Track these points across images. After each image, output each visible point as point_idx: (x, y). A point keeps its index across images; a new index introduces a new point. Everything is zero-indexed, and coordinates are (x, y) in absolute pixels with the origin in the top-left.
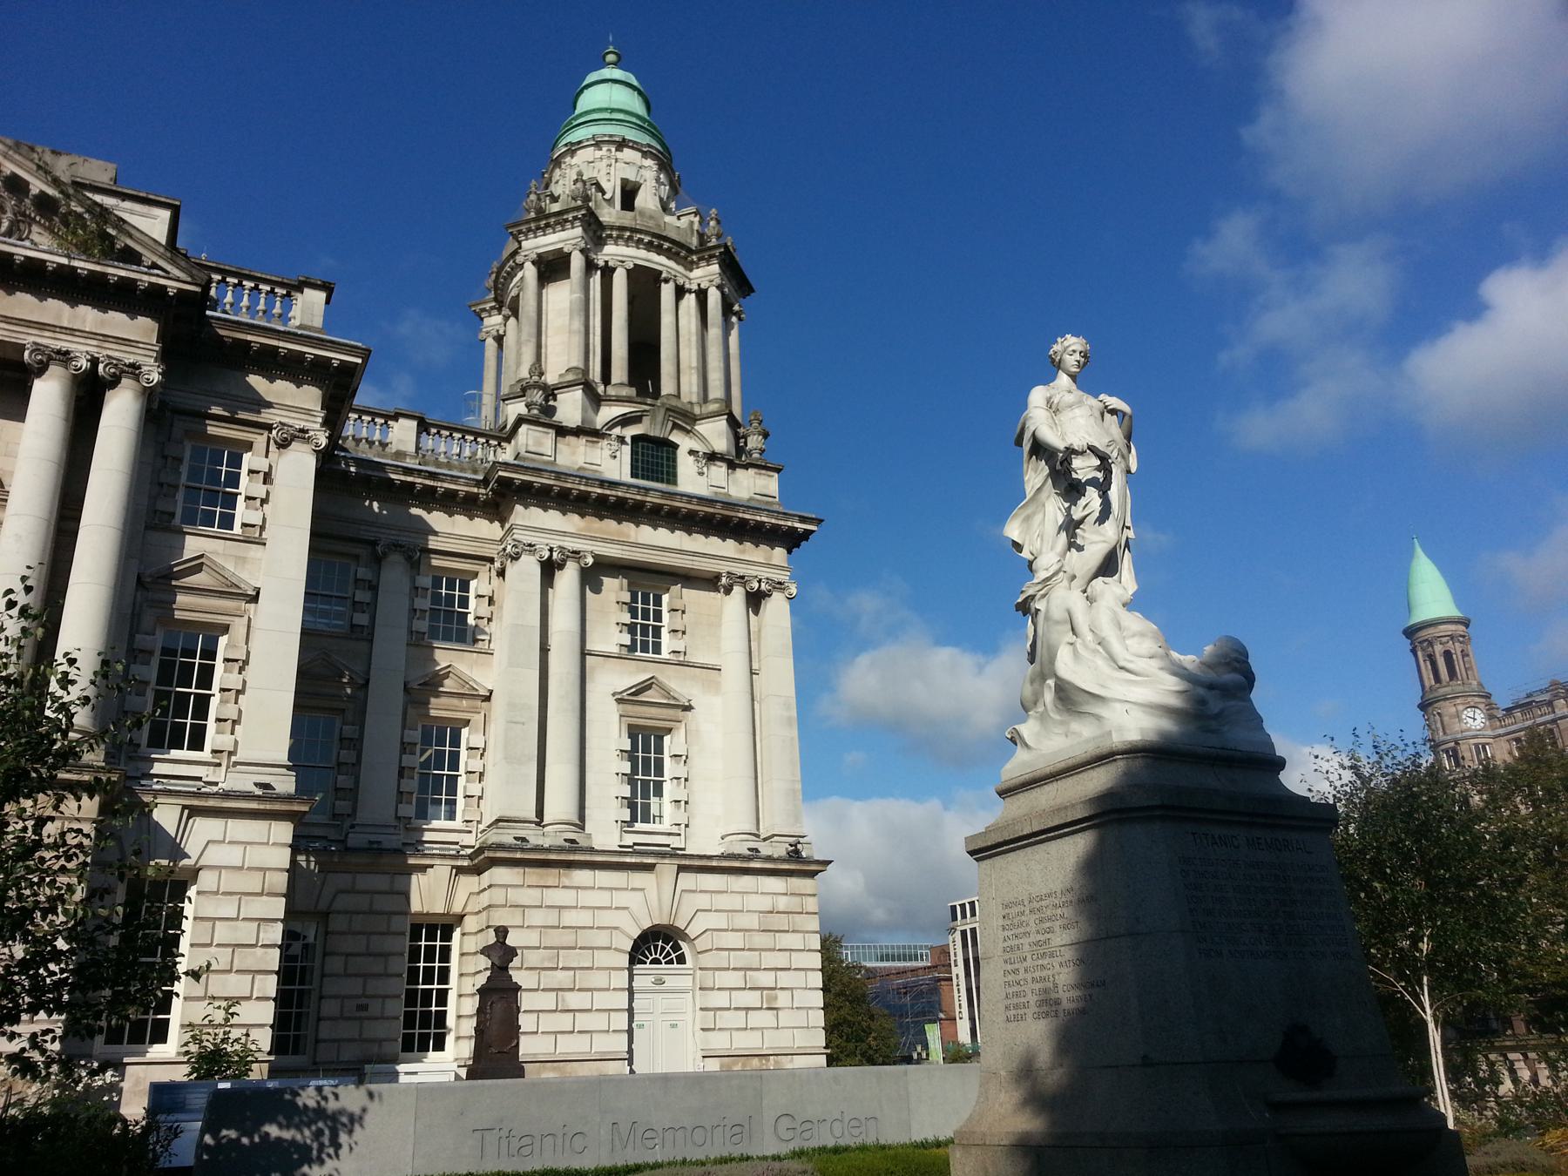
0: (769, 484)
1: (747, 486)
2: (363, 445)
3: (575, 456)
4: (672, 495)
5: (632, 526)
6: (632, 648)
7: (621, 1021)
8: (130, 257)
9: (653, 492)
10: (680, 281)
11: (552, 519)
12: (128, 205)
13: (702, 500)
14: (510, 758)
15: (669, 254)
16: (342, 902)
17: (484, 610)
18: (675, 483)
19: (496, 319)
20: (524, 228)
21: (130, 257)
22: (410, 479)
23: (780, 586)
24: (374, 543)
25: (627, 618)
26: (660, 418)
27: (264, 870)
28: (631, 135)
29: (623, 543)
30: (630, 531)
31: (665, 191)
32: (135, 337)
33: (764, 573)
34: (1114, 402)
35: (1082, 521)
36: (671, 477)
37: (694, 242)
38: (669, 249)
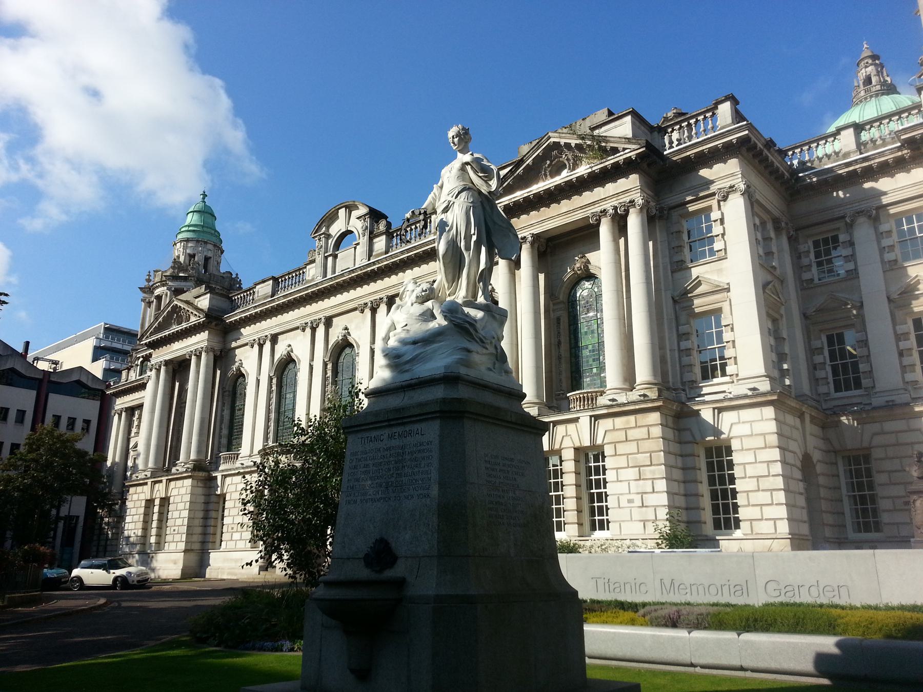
8: (615, 151)
12: (604, 129)
16: (877, 440)
21: (615, 151)
22: (851, 168)
24: (843, 217)
27: (764, 435)
32: (630, 186)
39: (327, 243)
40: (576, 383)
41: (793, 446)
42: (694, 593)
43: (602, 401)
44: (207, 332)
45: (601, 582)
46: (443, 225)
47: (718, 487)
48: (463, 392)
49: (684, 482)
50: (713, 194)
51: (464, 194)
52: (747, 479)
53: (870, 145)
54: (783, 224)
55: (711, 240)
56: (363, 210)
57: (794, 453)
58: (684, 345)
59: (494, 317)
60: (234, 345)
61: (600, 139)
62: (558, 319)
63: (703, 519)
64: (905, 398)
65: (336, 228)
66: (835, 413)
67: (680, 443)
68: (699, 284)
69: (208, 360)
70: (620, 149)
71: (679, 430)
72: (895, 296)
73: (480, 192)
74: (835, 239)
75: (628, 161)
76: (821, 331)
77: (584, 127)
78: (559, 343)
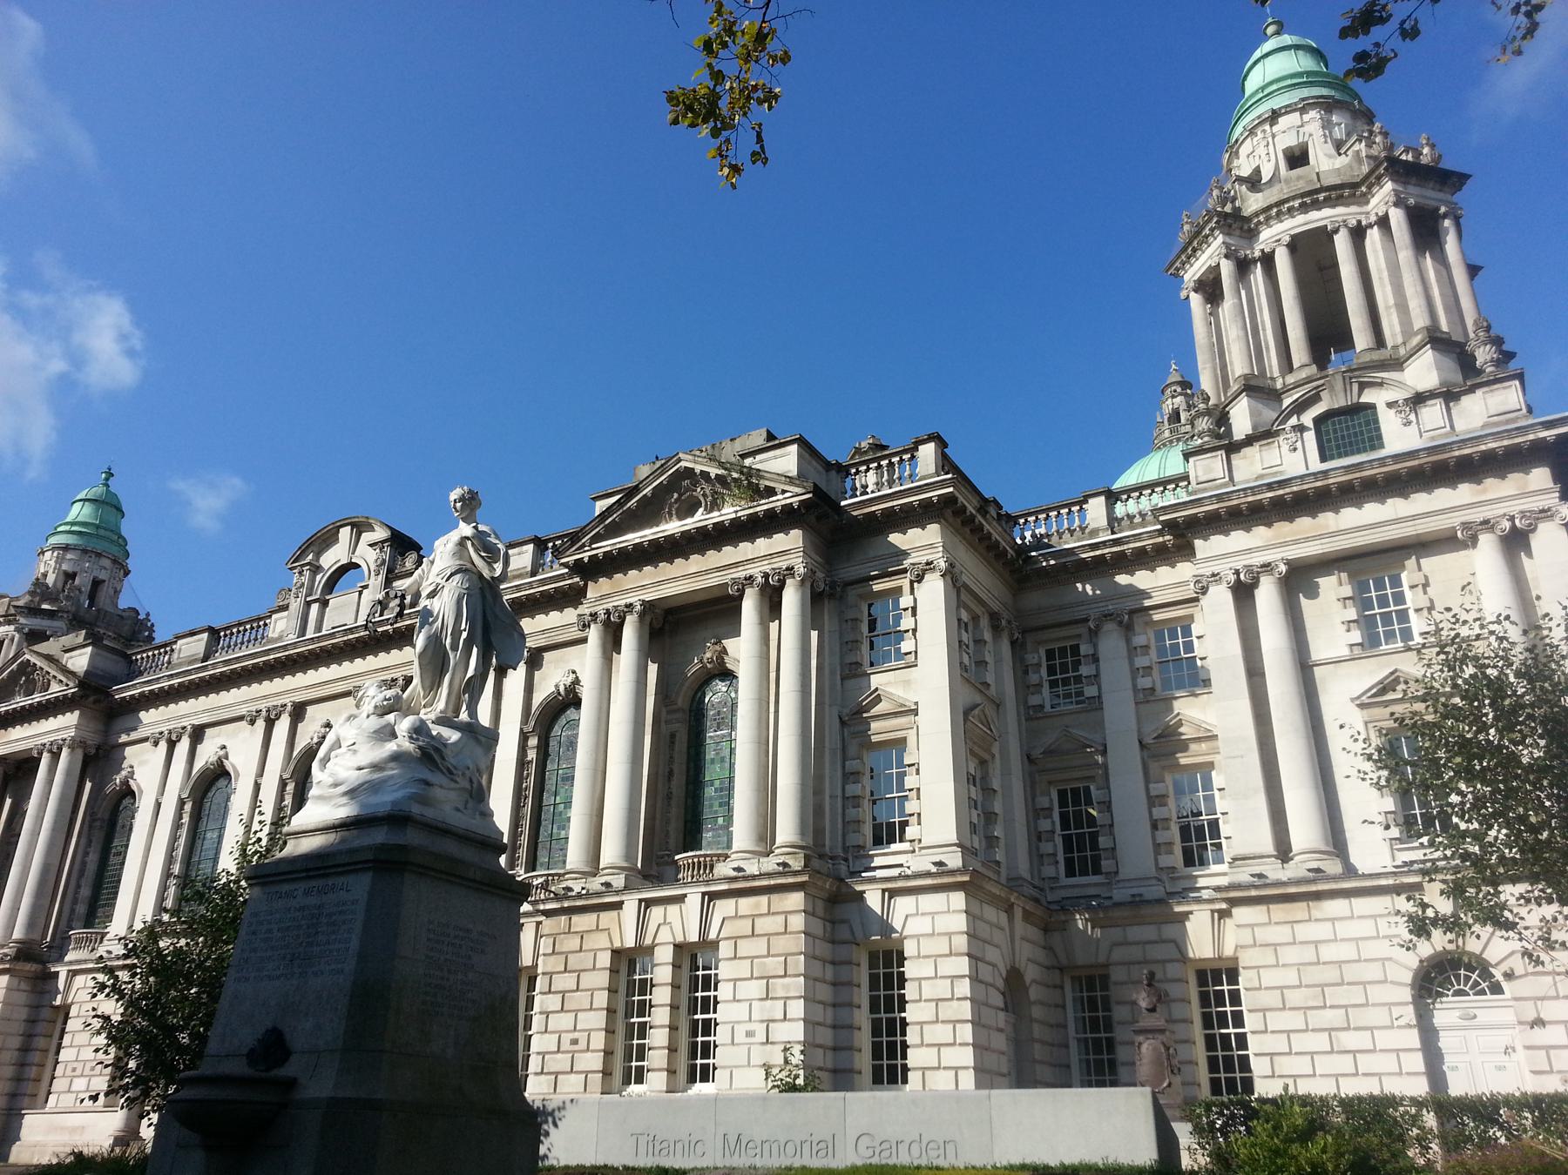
0: (1509, 397)
1: (1484, 412)
2: (1067, 536)
3: (1253, 466)
4: (1382, 461)
5: (1330, 515)
11: (1237, 540)
12: (759, 457)
15: (1330, 202)
16: (1118, 954)
18: (1382, 446)
21: (771, 492)
22: (1098, 553)
23: (1545, 514)
24: (1086, 620)
26: (1339, 385)
27: (950, 935)
29: (1321, 537)
32: (788, 546)
33: (1515, 507)
36: (1376, 441)
38: (1326, 199)
39: (312, 580)
40: (692, 838)
41: (992, 954)
42: (766, 1153)
43: (723, 869)
44: (77, 713)
45: (643, 1140)
46: (426, 615)
47: (883, 1015)
48: (412, 837)
49: (834, 1005)
50: (905, 571)
51: (457, 577)
52: (923, 1004)
53: (1126, 523)
54: (1004, 622)
55: (900, 635)
56: (380, 534)
57: (994, 966)
58: (852, 789)
59: (478, 741)
60: (124, 738)
61: (750, 473)
62: (673, 736)
63: (857, 1066)
64: (1155, 892)
65: (332, 558)
66: (1063, 909)
67: (833, 942)
68: (878, 700)
69: (71, 763)
70: (778, 490)
71: (833, 922)
72: (1148, 740)
73: (481, 576)
74: (1075, 650)
75: (788, 509)
76: (1050, 783)
77: (730, 452)
78: (671, 773)
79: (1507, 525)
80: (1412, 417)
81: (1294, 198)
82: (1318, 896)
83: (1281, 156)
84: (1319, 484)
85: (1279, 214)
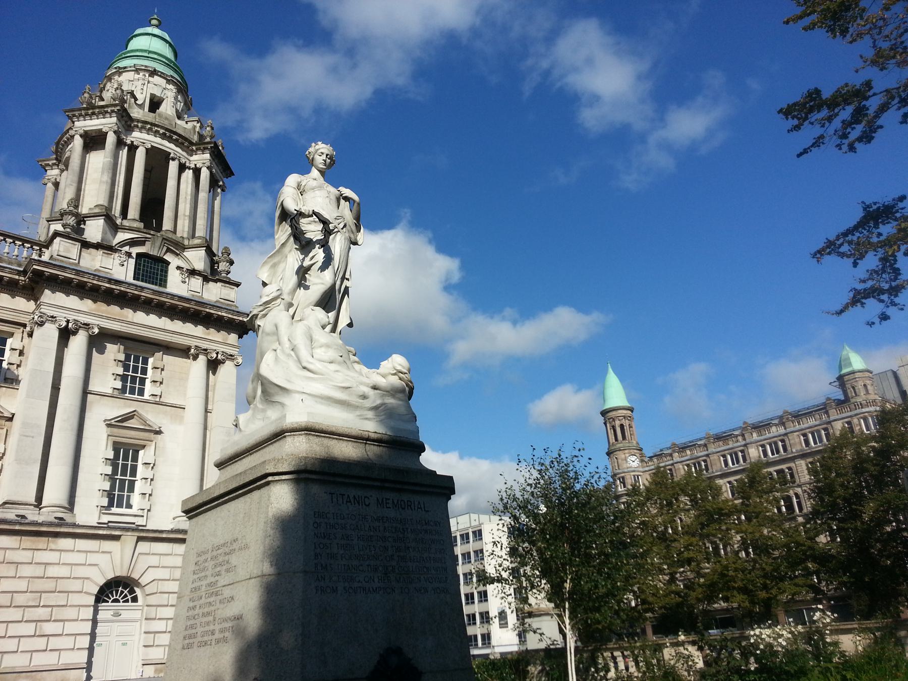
3: (93, 261)
4: (160, 293)
5: (131, 311)
6: (123, 390)
7: (85, 642)
9: (148, 290)
10: (183, 161)
11: (73, 301)
13: (181, 298)
14: (19, 460)
15: (176, 143)
17: (15, 359)
18: (165, 287)
19: (56, 172)
20: (77, 113)
23: (231, 357)
25: (120, 371)
28: (160, 68)
30: (128, 314)
31: (180, 106)
33: (221, 348)
34: (347, 192)
35: (309, 268)
36: (163, 282)
37: (195, 138)
38: (177, 140)
79: (214, 356)
80: (187, 280)
81: (162, 127)
82: (57, 535)
83: (148, 96)
84: (136, 292)
85: (150, 129)
